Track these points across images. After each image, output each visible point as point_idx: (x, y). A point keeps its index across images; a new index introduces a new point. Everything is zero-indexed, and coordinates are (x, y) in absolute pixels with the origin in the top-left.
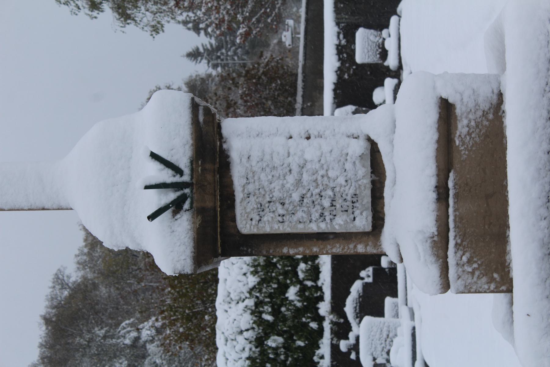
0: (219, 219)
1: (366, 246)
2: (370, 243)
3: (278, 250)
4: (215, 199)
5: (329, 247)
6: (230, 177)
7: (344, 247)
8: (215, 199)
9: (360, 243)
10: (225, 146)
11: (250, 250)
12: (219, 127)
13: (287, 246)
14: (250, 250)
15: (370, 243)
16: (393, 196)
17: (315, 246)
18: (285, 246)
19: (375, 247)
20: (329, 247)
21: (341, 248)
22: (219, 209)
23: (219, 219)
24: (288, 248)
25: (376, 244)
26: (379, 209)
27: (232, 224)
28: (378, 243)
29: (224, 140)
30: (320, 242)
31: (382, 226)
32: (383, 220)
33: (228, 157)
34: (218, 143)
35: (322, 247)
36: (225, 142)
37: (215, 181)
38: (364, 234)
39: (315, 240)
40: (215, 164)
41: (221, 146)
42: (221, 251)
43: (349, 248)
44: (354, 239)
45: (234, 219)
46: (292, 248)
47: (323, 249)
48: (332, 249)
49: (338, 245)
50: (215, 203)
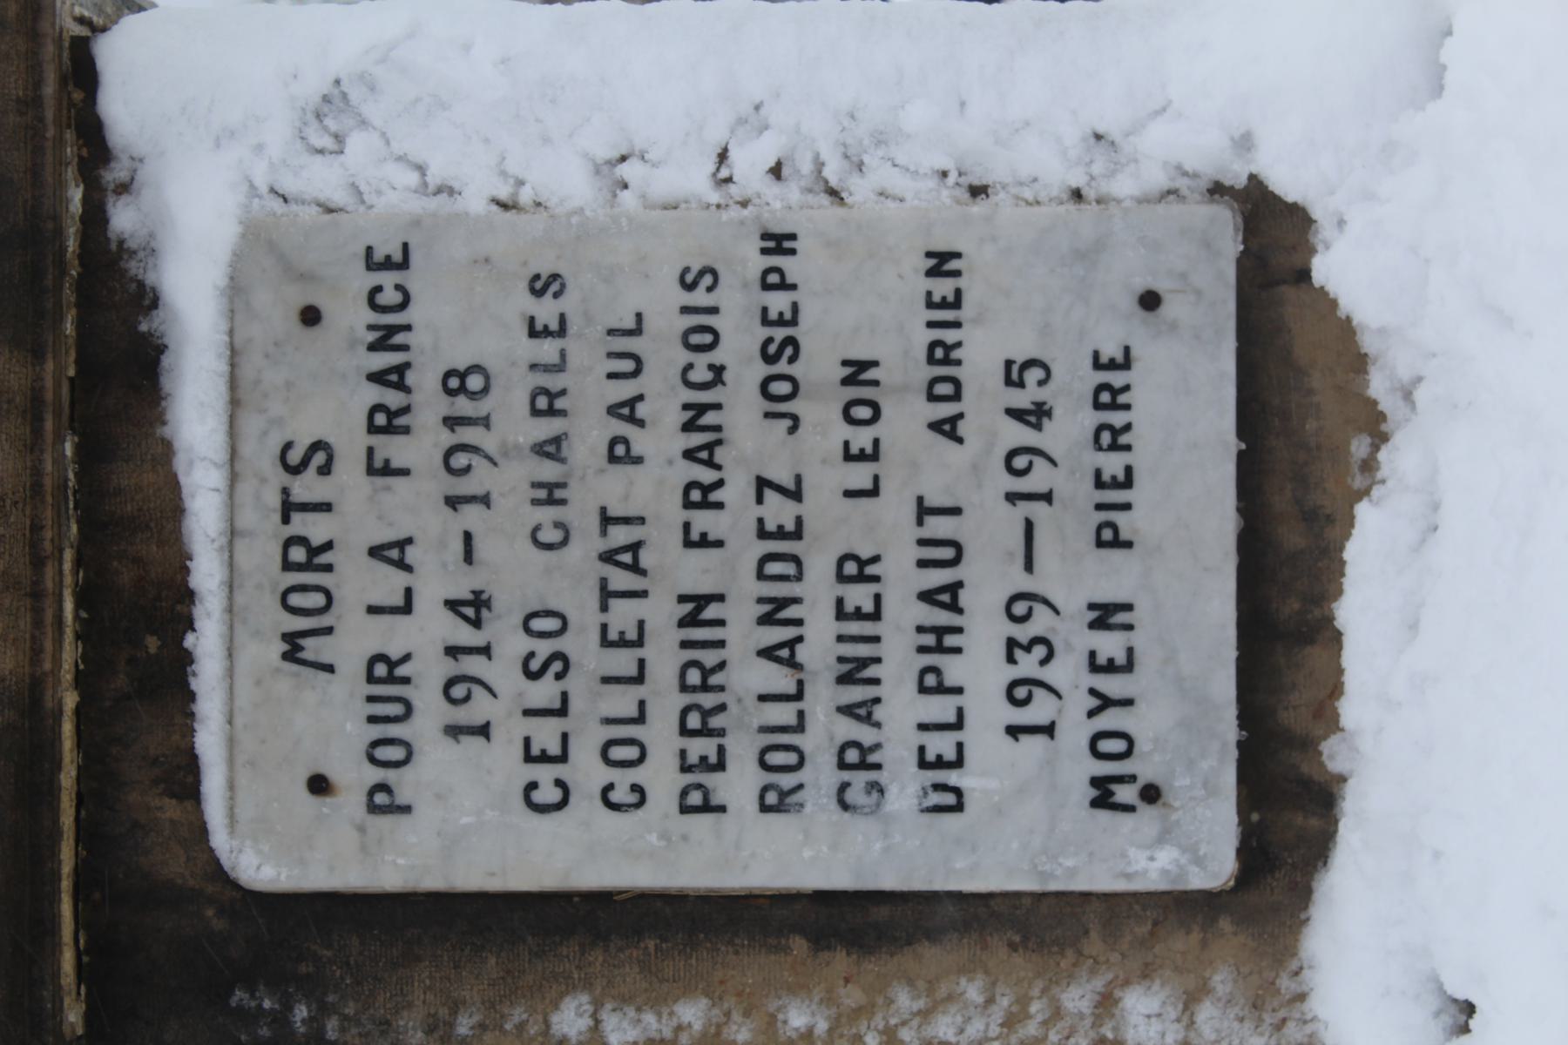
0: (68, 778)
1: (1190, 1001)
2: (1222, 981)
3: (518, 1014)
4: (38, 623)
5: (904, 1001)
6: (167, 450)
7: (1023, 1001)
8: (38, 623)
9: (1146, 974)
10: (123, 219)
11: (301, 1012)
12: (83, 73)
13: (587, 985)
14: (301, 1012)
15: (1222, 981)
16: (1413, 627)
17: (798, 989)
18: (570, 988)
19: (1256, 1005)
20: (904, 1001)
21: (998, 1013)
22: (70, 700)
23: (68, 778)
24: (598, 1005)
25: (1271, 987)
26: (1292, 717)
27: (171, 810)
28: (1286, 984)
29: (115, 173)
30: (840, 961)
31: (1317, 848)
32: (1322, 797)
33: (147, 299)
34: (76, 195)
35: (852, 996)
36: (124, 188)
37: (37, 488)
38: (1182, 908)
39: (799, 945)
40: (38, 355)
41: (95, 216)
42: (89, 1017)
43: (1057, 1013)
44: (1094, 944)
45: (183, 777)
46: (624, 1000)
47: (858, 1012)
48: (925, 1015)
49: (973, 991)
50: (36, 653)
